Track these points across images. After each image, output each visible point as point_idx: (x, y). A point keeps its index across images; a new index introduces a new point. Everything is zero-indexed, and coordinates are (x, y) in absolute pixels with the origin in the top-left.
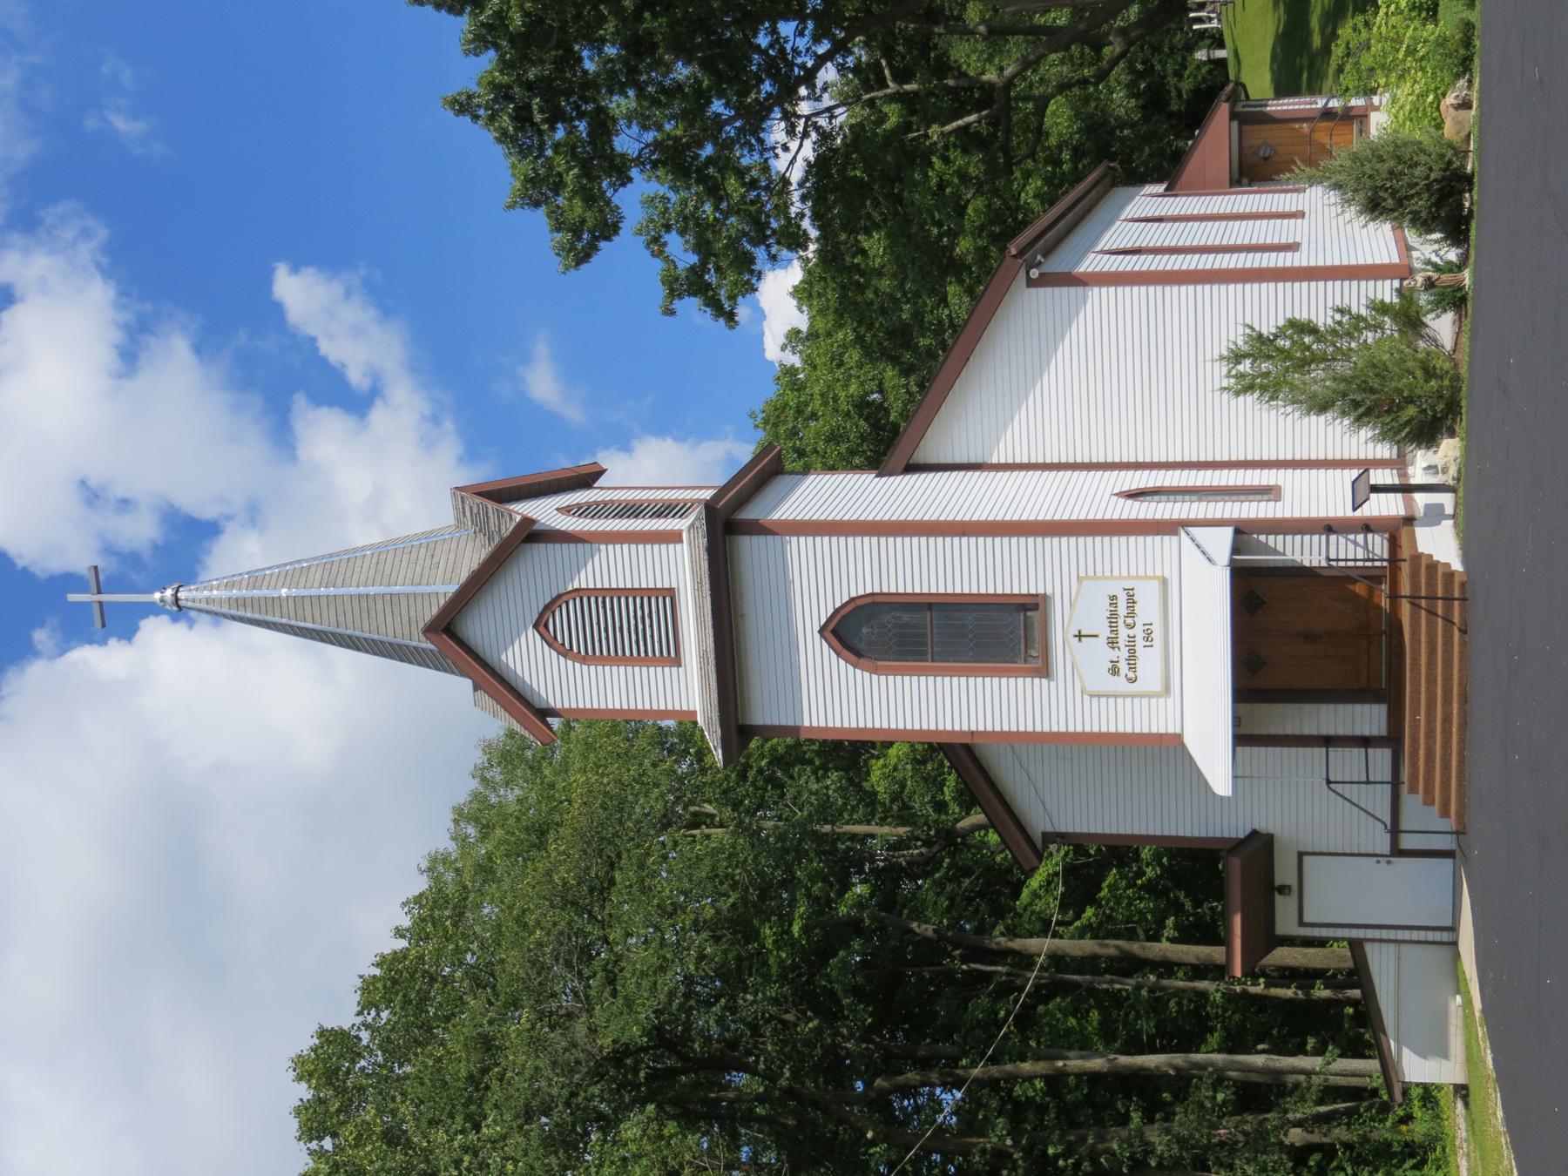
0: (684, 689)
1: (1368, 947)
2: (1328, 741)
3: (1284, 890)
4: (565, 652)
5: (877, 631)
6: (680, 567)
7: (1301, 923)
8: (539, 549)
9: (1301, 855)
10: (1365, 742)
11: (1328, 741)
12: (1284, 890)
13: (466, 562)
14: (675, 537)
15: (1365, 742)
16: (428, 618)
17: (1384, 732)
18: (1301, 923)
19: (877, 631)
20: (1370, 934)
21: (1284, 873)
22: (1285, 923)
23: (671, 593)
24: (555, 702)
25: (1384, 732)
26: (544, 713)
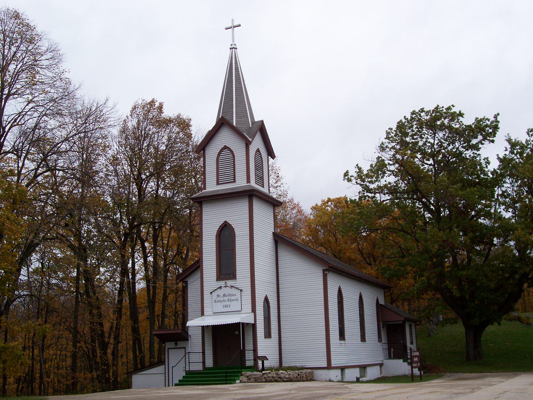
0: (212, 187)
1: (164, 366)
2: (204, 353)
3: (176, 344)
4: (219, 155)
5: (226, 233)
6: (241, 183)
7: (168, 349)
8: (243, 145)
9: (185, 348)
10: (204, 363)
11: (204, 353)
12: (176, 344)
13: (377, 389)
14: (248, 181)
15: (204, 363)
16: (225, 117)
17: (206, 366)
18: (168, 349)
19: (226, 233)
20: (167, 366)
21: (181, 344)
22: (169, 345)
23: (235, 181)
24: (207, 152)
25: (206, 366)
26: (204, 149)
